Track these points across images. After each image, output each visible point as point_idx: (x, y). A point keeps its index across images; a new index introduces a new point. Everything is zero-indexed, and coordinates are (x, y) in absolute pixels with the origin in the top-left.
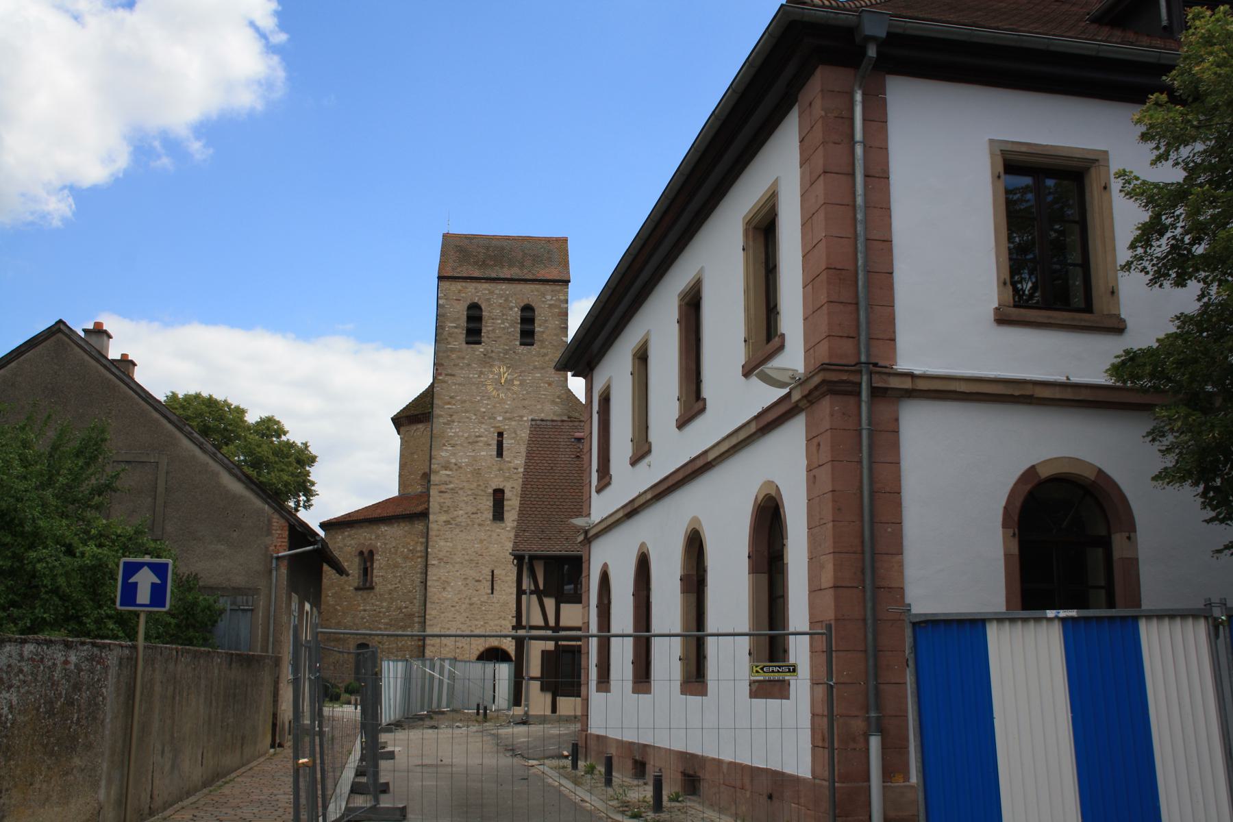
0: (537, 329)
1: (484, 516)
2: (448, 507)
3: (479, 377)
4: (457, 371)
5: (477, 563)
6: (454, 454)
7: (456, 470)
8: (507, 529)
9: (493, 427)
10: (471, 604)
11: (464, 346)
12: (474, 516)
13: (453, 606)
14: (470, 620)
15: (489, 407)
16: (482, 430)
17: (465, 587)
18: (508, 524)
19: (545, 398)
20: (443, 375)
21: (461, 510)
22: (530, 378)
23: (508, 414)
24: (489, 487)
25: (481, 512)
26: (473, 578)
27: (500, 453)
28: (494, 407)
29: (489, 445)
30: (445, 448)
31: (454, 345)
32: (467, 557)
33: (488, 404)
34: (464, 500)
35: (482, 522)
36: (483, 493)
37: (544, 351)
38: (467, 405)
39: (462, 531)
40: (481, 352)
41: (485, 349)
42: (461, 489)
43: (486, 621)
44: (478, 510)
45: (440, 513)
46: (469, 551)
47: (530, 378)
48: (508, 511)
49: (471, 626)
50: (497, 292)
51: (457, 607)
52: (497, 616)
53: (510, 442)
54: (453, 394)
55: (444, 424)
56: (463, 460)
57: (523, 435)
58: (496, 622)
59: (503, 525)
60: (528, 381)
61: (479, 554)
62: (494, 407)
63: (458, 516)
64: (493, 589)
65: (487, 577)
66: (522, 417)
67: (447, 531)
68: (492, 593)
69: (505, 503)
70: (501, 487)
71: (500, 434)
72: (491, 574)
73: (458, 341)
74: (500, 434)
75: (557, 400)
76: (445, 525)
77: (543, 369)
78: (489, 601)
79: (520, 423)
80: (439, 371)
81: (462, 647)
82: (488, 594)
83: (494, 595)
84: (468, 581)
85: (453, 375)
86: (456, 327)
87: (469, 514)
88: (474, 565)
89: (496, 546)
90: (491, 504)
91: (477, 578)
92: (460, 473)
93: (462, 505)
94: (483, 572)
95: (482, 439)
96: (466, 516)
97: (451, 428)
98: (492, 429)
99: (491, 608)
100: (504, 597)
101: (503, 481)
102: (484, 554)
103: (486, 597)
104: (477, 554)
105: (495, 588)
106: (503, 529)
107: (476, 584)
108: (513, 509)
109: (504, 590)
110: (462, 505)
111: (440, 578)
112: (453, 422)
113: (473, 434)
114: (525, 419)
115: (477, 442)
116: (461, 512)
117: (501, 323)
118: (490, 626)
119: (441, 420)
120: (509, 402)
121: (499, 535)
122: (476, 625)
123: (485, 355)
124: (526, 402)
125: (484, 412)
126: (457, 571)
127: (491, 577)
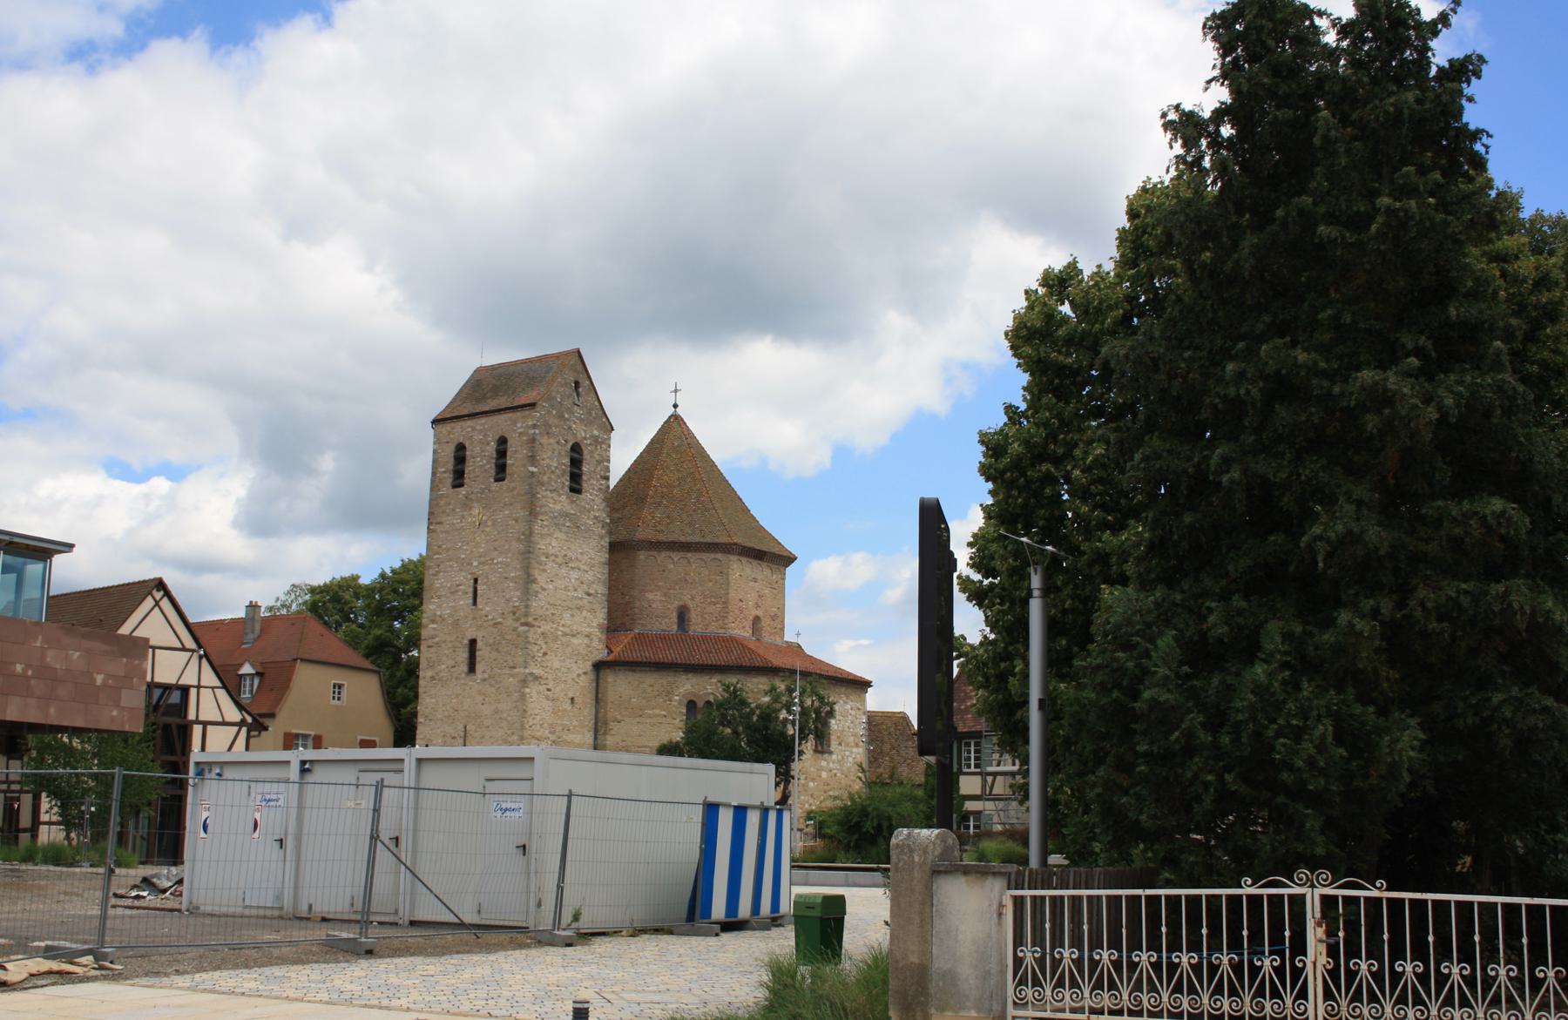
0: (509, 462)
3: (461, 522)
4: (444, 519)
6: (439, 606)
11: (451, 490)
12: (452, 670)
28: (472, 552)
32: (446, 713)
33: (467, 550)
37: (513, 485)
38: (451, 553)
50: (478, 427)
62: (472, 552)
66: (493, 560)
71: (476, 580)
73: (446, 489)
74: (476, 580)
77: (511, 504)
85: (440, 523)
86: (444, 472)
93: (444, 659)
95: (461, 587)
110: (444, 659)
115: (457, 591)
119: (431, 572)
124: (497, 543)
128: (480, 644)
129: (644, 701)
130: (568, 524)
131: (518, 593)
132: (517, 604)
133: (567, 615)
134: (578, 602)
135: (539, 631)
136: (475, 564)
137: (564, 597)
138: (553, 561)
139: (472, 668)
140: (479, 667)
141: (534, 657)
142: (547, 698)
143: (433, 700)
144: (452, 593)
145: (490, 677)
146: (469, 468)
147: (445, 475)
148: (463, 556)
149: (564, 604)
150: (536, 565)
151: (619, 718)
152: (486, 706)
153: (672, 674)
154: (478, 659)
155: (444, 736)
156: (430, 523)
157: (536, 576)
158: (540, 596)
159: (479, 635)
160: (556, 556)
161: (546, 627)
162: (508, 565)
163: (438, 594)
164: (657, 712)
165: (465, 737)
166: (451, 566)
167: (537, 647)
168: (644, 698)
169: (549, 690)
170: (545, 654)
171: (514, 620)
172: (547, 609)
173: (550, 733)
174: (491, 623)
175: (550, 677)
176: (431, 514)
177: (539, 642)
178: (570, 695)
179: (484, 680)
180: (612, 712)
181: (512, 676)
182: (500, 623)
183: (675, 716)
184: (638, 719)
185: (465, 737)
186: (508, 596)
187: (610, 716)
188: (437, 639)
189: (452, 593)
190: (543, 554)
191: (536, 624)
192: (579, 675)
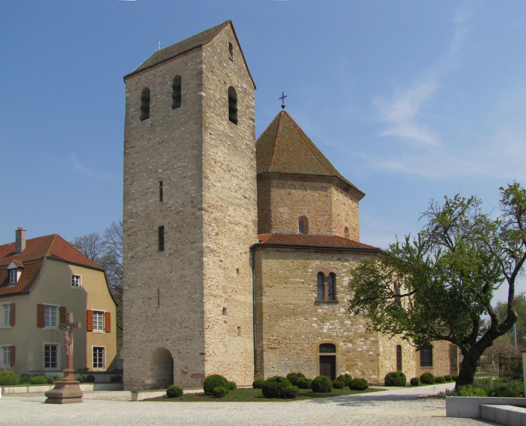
2: (133, 246)
3: (148, 142)
5: (149, 285)
7: (136, 217)
9: (156, 179)
10: (147, 317)
11: (140, 122)
12: (146, 250)
13: (137, 319)
14: (146, 328)
15: (154, 164)
16: (150, 183)
19: (188, 146)
20: (128, 149)
21: (140, 246)
22: (178, 133)
23: (165, 166)
24: (155, 226)
25: (151, 246)
26: (147, 297)
27: (161, 199)
29: (154, 193)
30: (130, 202)
31: (134, 124)
33: (153, 162)
34: (141, 239)
36: (151, 231)
40: (150, 123)
41: (151, 121)
42: (139, 231)
43: (156, 329)
44: (149, 244)
45: (128, 251)
47: (178, 133)
51: (139, 320)
53: (167, 187)
54: (133, 161)
55: (129, 184)
56: (140, 209)
57: (175, 180)
59: (163, 253)
60: (177, 136)
61: (150, 277)
62: (157, 163)
63: (138, 252)
64: (159, 303)
66: (173, 165)
67: (132, 264)
70: (162, 224)
71: (161, 183)
72: (157, 292)
73: (137, 122)
74: (161, 183)
75: (196, 145)
76: (131, 259)
79: (173, 170)
80: (126, 146)
81: (143, 349)
82: (157, 308)
83: (160, 309)
85: (133, 147)
86: (135, 111)
88: (148, 286)
89: (160, 270)
91: (150, 297)
92: (139, 219)
94: (153, 291)
95: (150, 190)
97: (133, 187)
98: (156, 181)
100: (166, 309)
101: (163, 220)
103: (155, 310)
106: (163, 257)
107: (149, 301)
111: (129, 299)
112: (134, 182)
113: (145, 187)
114: (176, 166)
115: (147, 193)
117: (161, 97)
118: (158, 332)
120: (165, 157)
121: (161, 262)
122: (150, 332)
123: (151, 125)
125: (151, 169)
126: (138, 293)
127: (157, 295)
128: (166, 229)
129: (288, 272)
130: (229, 143)
131: (195, 187)
132: (194, 195)
133: (231, 209)
134: (238, 201)
135: (212, 216)
136: (160, 171)
137: (229, 195)
138: (220, 167)
139: (161, 248)
140: (167, 246)
141: (209, 235)
142: (220, 267)
143: (134, 273)
144: (144, 195)
145: (175, 251)
146: (152, 105)
147: (136, 113)
148: (151, 167)
149: (230, 200)
150: (209, 167)
151: (271, 284)
152: (173, 274)
153: (306, 253)
154: (165, 240)
155: (143, 298)
156: (126, 149)
157: (208, 175)
158: (211, 190)
159: (165, 223)
160: (222, 164)
161: (217, 214)
162: (185, 167)
163: (134, 197)
164: (298, 280)
165: (159, 297)
166: (142, 176)
167: (211, 228)
169: (221, 261)
170: (217, 234)
171: (192, 207)
172: (217, 202)
173: (223, 292)
174: (174, 212)
175: (221, 251)
176: (126, 142)
177: (212, 225)
178: (236, 267)
179: (171, 254)
180: (266, 281)
181: (193, 249)
182: (181, 211)
183: (309, 283)
184: (284, 285)
185: (159, 297)
186: (186, 191)
187: (264, 282)
188: (135, 229)
189: (144, 195)
190: (213, 159)
191: (210, 210)
192: (241, 254)
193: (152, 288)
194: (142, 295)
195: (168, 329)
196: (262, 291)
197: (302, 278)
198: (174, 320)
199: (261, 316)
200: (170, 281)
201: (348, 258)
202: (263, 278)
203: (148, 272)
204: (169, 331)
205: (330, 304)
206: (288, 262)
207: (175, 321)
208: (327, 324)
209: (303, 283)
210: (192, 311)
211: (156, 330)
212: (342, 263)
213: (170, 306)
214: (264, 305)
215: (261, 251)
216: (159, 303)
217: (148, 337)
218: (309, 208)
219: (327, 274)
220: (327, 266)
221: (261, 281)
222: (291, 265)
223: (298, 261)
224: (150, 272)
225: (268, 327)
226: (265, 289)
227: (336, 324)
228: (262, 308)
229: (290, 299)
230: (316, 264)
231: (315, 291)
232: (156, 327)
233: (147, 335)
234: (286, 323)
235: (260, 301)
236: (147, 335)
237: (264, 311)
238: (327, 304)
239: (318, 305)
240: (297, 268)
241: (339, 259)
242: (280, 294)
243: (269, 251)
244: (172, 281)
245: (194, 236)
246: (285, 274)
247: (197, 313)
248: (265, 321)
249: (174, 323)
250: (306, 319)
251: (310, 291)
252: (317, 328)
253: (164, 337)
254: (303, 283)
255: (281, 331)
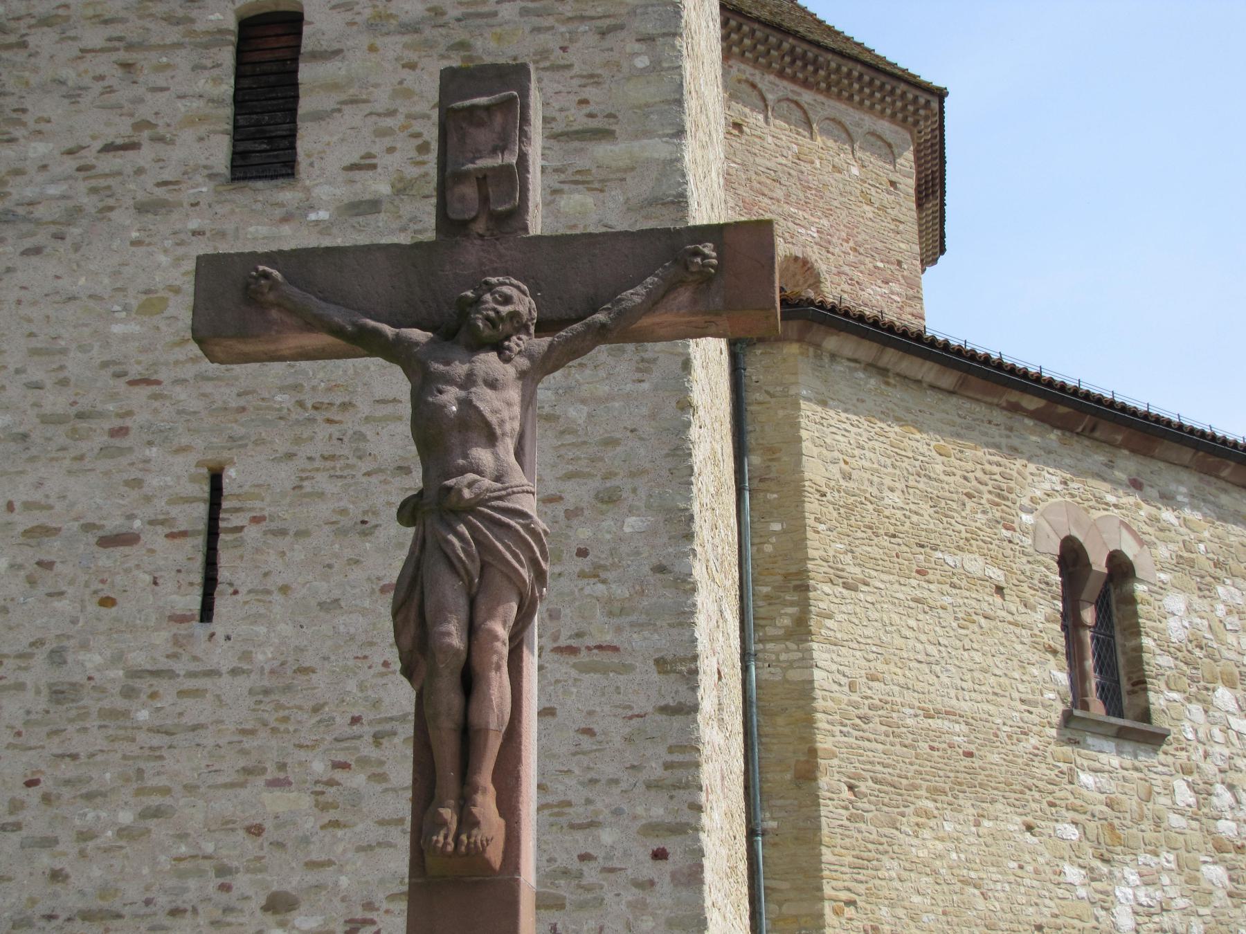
1: (176, 154)
8: (313, 216)
17: (32, 581)
18: (323, 192)
26: (88, 527)
32: (55, 402)
35: (161, 193)
39: (37, 251)
43: (155, 800)
46: (75, 365)
48: (318, 116)
49: (49, 843)
52: (231, 765)
58: (225, 805)
61: (135, 371)
64: (210, 582)
65: (174, 511)
68: (207, 613)
69: (306, 72)
72: (204, 490)
78: (180, 667)
82: (182, 619)
83: (219, 625)
84: (53, 549)
87: (89, 157)
88: (101, 439)
90: (227, 88)
91: (113, 524)
94: (153, 481)
96: (71, 164)
99: (196, 710)
100: (286, 629)
102: (163, 375)
103: (162, 638)
104: (117, 375)
105: (223, 574)
107: (107, 559)
108: (354, 101)
109: (284, 589)
116: (38, 149)
118: (182, 837)
122: (84, 836)
127: (202, 510)
129: (926, 509)
153: (999, 416)
164: (975, 564)
165: (213, 533)
168: (928, 497)
185: (213, 533)
193: (153, 452)
194: (28, 506)
195: (306, 801)
196: (805, 606)
197: (994, 560)
198: (366, 730)
199: (807, 774)
200: (345, 406)
201: (1173, 487)
202: (810, 521)
203: (117, 329)
204: (309, 824)
205: (1128, 747)
206: (921, 443)
207: (377, 738)
208: (1127, 870)
209: (999, 590)
210: (572, 650)
211: (157, 813)
212: (1154, 511)
213: (331, 606)
214: (819, 704)
215: (793, 349)
216: (210, 582)
217: (57, 876)
218: (824, 222)
219: (1099, 563)
220: (1096, 514)
221: (796, 535)
222: (939, 468)
223: (968, 453)
224: (134, 328)
225: (848, 859)
226: (824, 595)
227: (1165, 880)
228: (809, 722)
229: (944, 679)
230: (1047, 486)
231: (1054, 652)
232: (166, 791)
233: (45, 860)
234: (940, 846)
235: (794, 675)
236: (45, 860)
237: (824, 743)
238: (1109, 745)
239: (1077, 743)
240: (969, 496)
241: (1136, 485)
242: (899, 641)
243: (833, 357)
244: (364, 408)
245: (590, 92)
246: (915, 518)
247: (626, 668)
248: (831, 814)
249: (368, 750)
250: (1029, 828)
251: (1035, 645)
252: (1082, 892)
253: (242, 882)
254: (999, 590)
255: (916, 899)
